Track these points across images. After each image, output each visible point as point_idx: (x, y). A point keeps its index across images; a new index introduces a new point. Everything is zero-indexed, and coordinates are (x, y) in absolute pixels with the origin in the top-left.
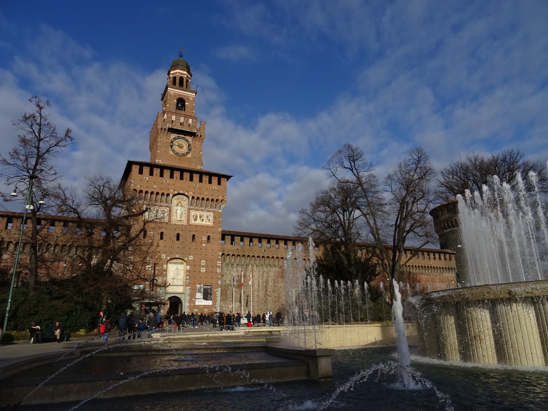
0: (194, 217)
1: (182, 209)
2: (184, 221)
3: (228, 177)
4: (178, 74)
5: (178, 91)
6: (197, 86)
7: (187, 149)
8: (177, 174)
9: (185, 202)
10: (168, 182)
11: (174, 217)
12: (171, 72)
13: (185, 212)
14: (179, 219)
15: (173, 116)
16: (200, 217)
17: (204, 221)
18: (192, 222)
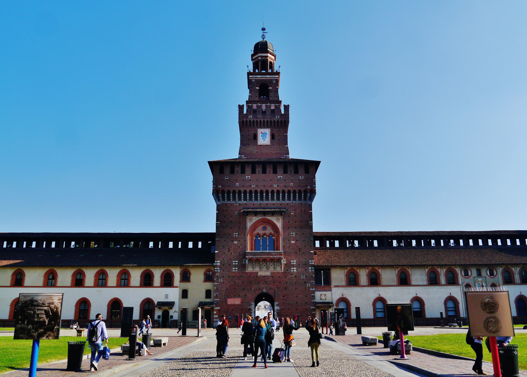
3: (316, 164)
4: (260, 58)
10: (249, 178)
12: (254, 58)
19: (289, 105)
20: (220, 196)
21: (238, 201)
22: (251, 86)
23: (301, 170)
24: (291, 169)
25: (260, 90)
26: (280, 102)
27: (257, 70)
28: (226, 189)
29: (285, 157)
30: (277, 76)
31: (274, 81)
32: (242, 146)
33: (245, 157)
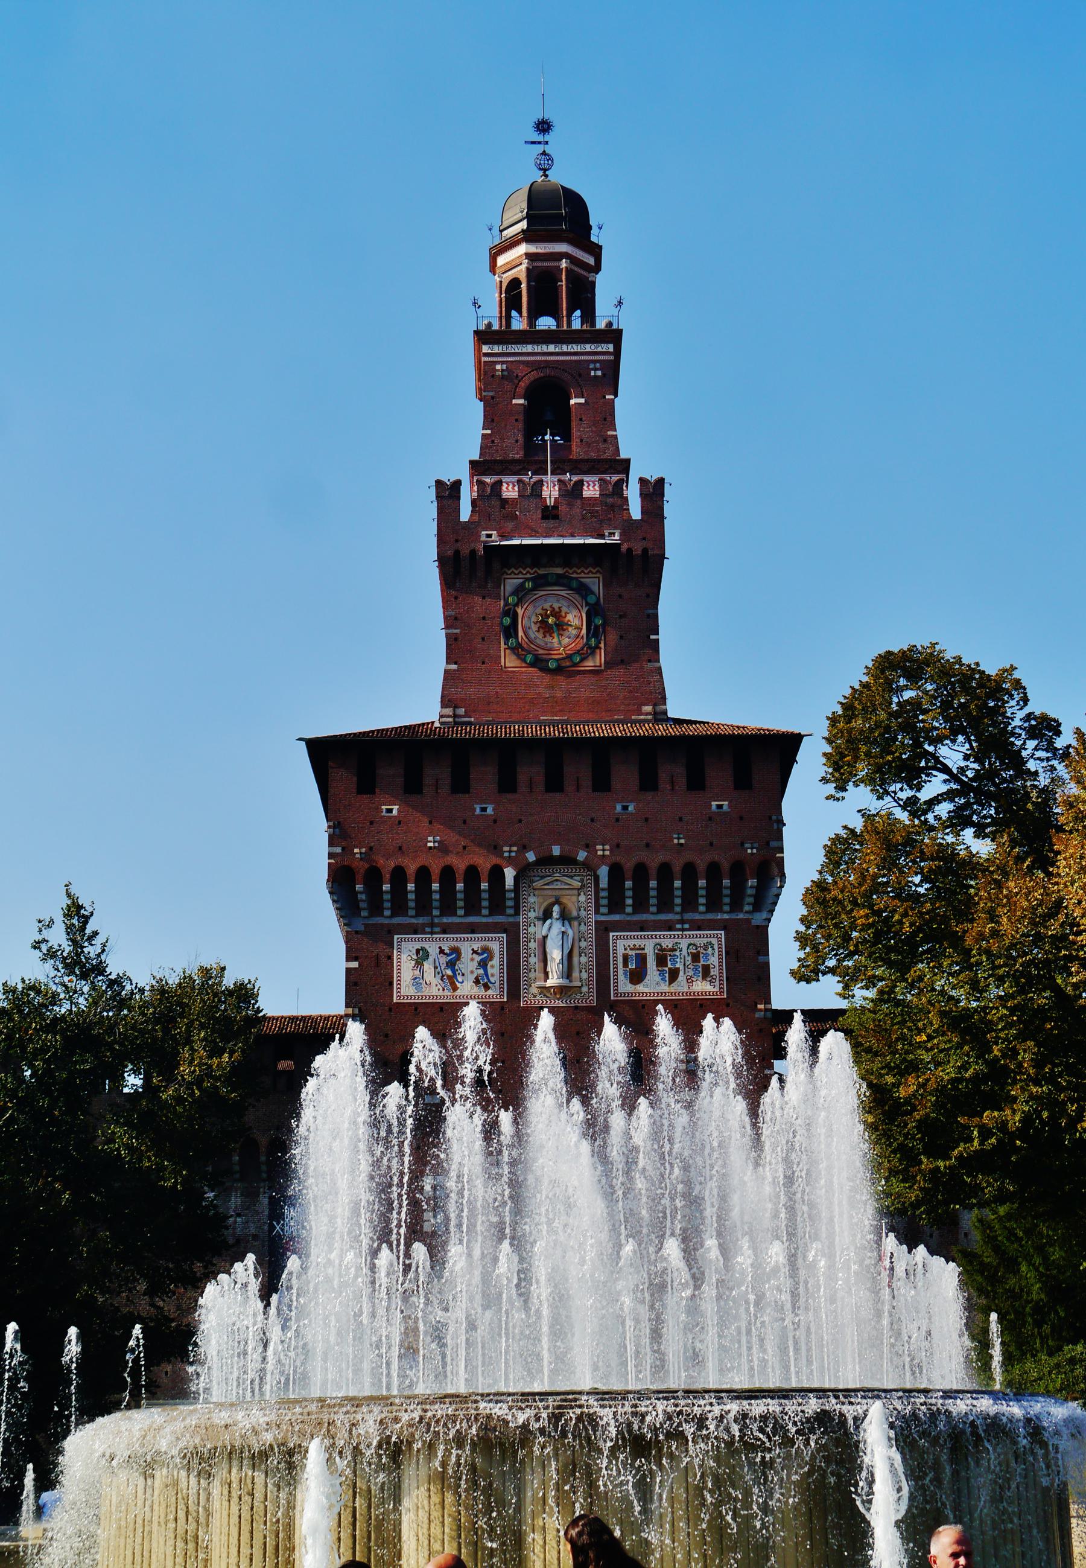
0: (632, 966)
1: (570, 932)
2: (585, 989)
5: (529, 348)
6: (620, 303)
7: (584, 631)
8: (530, 772)
9: (582, 898)
10: (490, 811)
11: (532, 975)
12: (501, 260)
13: (583, 944)
14: (553, 981)
15: (505, 479)
16: (661, 960)
17: (682, 977)
18: (623, 986)
19: (661, 482)
20: (361, 893)
21: (442, 915)
22: (491, 394)
23: (718, 774)
24: (672, 771)
25: (527, 410)
26: (624, 466)
27: (514, 313)
28: (387, 865)
29: (647, 714)
30: (611, 348)
31: (596, 369)
32: (454, 667)
33: (467, 715)
